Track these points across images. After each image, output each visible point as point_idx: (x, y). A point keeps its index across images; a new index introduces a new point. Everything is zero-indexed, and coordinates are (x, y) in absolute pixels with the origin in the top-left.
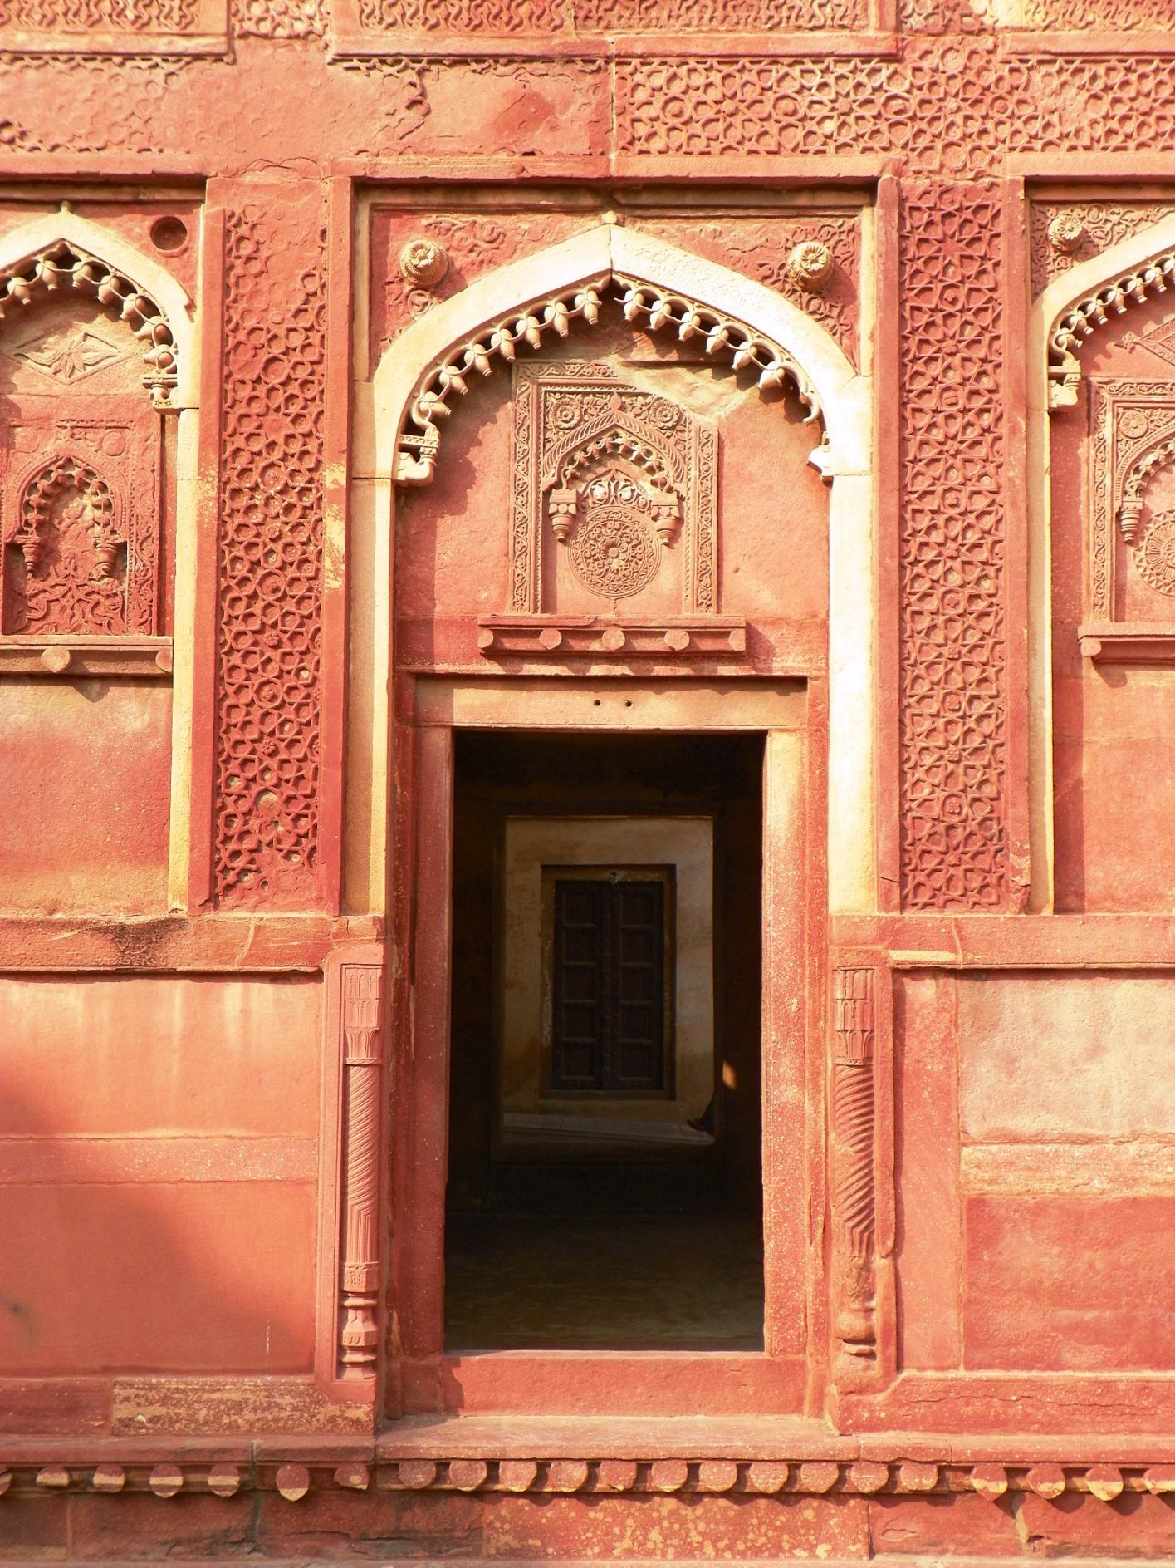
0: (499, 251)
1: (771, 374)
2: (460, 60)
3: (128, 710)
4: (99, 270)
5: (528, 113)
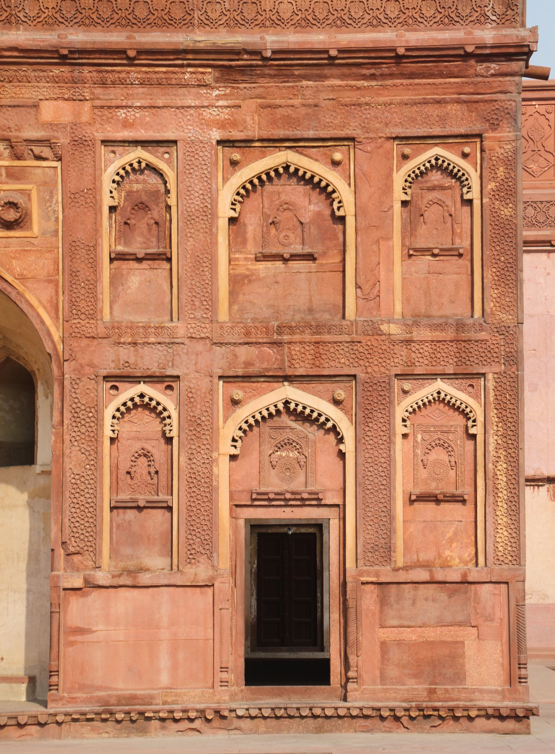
1: (329, 425)
3: (159, 515)
4: (151, 399)
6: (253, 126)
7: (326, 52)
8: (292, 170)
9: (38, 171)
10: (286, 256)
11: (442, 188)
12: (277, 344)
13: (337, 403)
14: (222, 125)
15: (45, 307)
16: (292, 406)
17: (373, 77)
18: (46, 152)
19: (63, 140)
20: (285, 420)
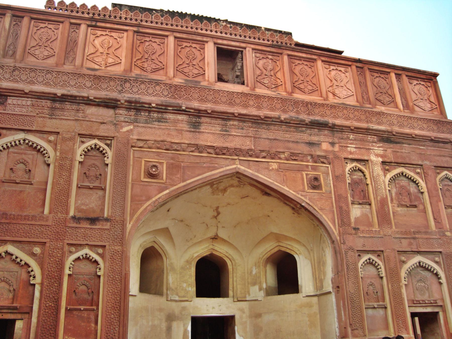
0: (409, 259)
2: (404, 238)
3: (381, 312)
4: (373, 260)
5: (410, 244)
6: (391, 157)
7: (411, 135)
8: (404, 174)
9: (322, 168)
10: (408, 205)
11: (449, 185)
12: (414, 238)
13: (437, 262)
14: (382, 156)
15: (330, 221)
16: (421, 264)
17: (424, 146)
18: (325, 161)
19: (331, 156)
20: (419, 270)
